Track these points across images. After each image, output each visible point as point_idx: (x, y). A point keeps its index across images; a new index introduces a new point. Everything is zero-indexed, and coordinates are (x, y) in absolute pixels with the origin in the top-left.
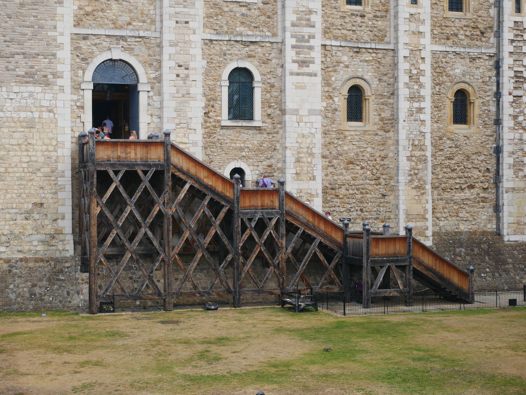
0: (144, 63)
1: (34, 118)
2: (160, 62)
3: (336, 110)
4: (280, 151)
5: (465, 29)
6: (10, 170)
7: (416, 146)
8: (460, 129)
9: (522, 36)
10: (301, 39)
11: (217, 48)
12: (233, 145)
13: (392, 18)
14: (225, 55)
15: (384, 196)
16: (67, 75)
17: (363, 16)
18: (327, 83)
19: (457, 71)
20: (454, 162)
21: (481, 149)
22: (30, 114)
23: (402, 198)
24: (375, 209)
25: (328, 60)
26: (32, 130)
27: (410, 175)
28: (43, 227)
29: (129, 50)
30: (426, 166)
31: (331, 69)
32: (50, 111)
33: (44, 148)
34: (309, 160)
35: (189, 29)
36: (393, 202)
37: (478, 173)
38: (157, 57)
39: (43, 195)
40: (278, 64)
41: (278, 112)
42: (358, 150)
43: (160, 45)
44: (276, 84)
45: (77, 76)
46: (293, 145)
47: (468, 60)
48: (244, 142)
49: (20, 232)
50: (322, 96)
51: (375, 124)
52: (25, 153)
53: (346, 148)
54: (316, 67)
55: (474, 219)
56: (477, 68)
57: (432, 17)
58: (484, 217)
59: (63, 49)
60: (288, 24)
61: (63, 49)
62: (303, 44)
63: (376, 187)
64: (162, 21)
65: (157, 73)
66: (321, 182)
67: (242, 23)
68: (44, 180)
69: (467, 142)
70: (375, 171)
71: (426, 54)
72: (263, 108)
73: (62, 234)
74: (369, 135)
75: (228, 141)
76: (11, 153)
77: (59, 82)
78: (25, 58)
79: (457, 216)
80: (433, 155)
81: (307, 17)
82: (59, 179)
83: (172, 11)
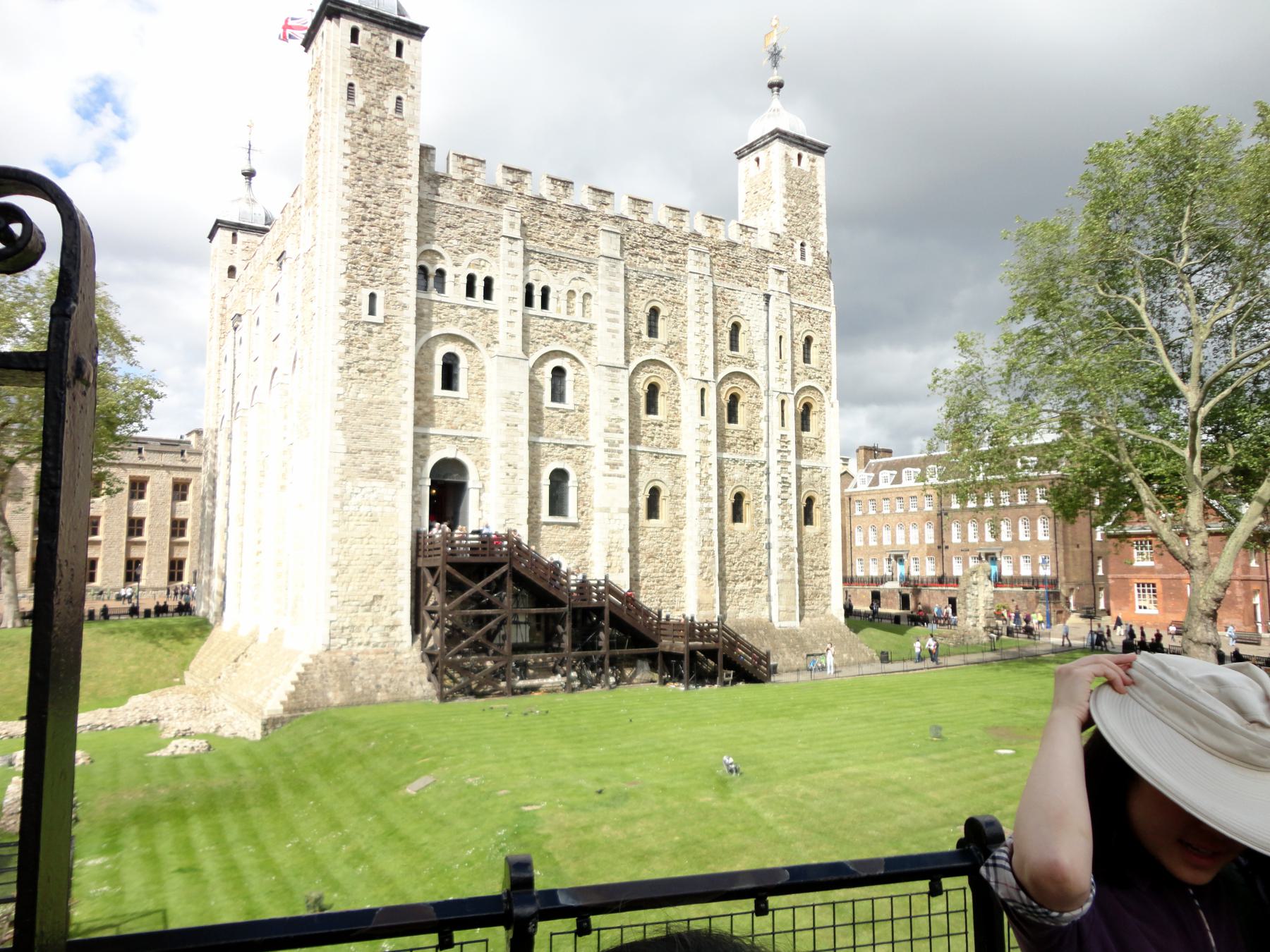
15: (678, 587)
18: (633, 484)
32: (393, 506)
34: (618, 554)
53: (646, 543)
54: (625, 470)
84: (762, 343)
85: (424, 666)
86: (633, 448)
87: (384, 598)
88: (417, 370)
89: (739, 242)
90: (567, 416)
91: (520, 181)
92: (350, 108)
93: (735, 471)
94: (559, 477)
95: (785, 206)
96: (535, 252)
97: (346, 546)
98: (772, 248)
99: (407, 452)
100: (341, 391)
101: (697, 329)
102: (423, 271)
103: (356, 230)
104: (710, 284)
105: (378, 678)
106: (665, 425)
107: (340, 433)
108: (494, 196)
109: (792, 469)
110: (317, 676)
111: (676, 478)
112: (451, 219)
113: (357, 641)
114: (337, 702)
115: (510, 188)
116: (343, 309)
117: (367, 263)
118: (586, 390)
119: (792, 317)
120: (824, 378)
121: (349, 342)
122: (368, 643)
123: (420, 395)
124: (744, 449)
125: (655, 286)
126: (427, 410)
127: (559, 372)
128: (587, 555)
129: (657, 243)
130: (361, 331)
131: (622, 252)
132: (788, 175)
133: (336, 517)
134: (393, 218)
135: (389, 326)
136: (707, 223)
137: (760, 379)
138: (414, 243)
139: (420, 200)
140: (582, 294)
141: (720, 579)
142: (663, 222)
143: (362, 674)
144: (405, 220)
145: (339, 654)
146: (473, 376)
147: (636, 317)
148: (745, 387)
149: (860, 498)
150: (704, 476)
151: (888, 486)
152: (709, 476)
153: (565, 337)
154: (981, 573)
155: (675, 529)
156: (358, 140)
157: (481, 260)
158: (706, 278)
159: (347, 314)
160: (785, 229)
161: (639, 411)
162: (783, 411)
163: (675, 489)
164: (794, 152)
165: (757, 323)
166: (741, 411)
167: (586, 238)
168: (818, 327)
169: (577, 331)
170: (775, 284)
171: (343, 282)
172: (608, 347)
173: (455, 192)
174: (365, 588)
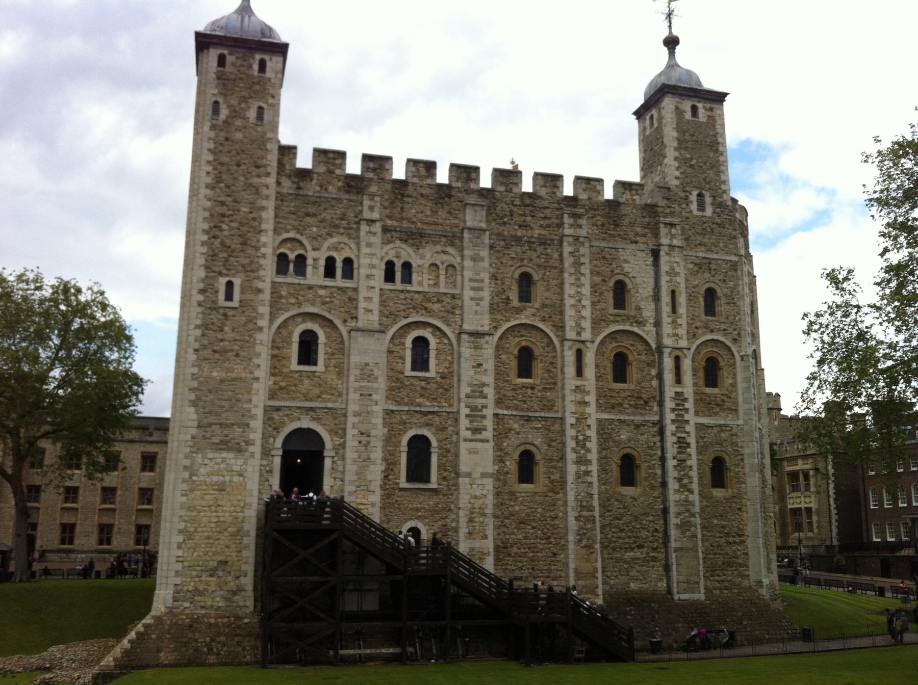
0: (330, 431)
1: (225, 482)
2: (344, 430)
3: (507, 473)
4: (454, 512)
5: (629, 399)
6: (200, 529)
7: (584, 506)
8: (629, 491)
9: (683, 405)
10: (474, 408)
11: (398, 417)
12: (410, 506)
13: (560, 390)
14: (405, 423)
15: (555, 555)
16: (258, 443)
17: (533, 388)
18: (498, 448)
19: (622, 437)
20: (622, 522)
21: (649, 511)
22: (221, 478)
23: (572, 557)
24: (546, 568)
25: (500, 427)
26: (222, 492)
27: (578, 535)
28: (226, 583)
29: (318, 420)
30: (595, 525)
31: (503, 436)
32: (241, 475)
33: (232, 509)
34: (481, 519)
35: (371, 400)
36: (563, 561)
37: (647, 533)
38: (342, 426)
39: (228, 554)
40: (454, 432)
41: (453, 475)
42: (529, 511)
43: (345, 415)
44: (451, 449)
45: (269, 443)
46: (466, 505)
47: (632, 427)
49: (204, 589)
50: (494, 460)
51: (546, 486)
52: (215, 514)
53: (517, 508)
54: (488, 434)
55: (645, 578)
56: (642, 434)
57: (597, 388)
59: (256, 419)
60: (463, 396)
61: (256, 419)
62: (476, 413)
63: (547, 546)
64: (347, 394)
65: (342, 440)
66: (492, 540)
67: (422, 395)
68: (231, 539)
69: (635, 503)
70: (545, 530)
71: (592, 421)
72: (438, 471)
73: (244, 590)
74: (540, 496)
75: (405, 502)
76: (202, 514)
77: (251, 449)
78: (221, 427)
79: (628, 575)
80: (600, 516)
81: (481, 389)
82: (244, 538)
83: (357, 385)
84: (651, 299)
87: (229, 563)
88: (273, 348)
89: (622, 200)
90: (428, 383)
91: (381, 167)
92: (215, 122)
93: (622, 432)
94: (419, 446)
95: (676, 159)
99: (257, 424)
100: (195, 370)
102: (282, 259)
103: (215, 227)
104: (587, 245)
107: (192, 410)
108: (354, 184)
109: (691, 428)
112: (312, 209)
115: (371, 175)
116: (201, 298)
117: (225, 255)
120: (730, 330)
121: (205, 326)
122: (212, 606)
126: (283, 384)
127: (421, 344)
129: (527, 210)
130: (215, 317)
131: (488, 222)
132: (680, 127)
134: (251, 212)
135: (244, 309)
136: (584, 186)
138: (271, 233)
140: (445, 266)
144: (264, 215)
146: (330, 351)
147: (503, 283)
148: (632, 345)
150: (581, 438)
153: (426, 309)
155: (550, 494)
156: (220, 148)
157: (340, 243)
158: (581, 240)
159: (204, 301)
160: (677, 182)
161: (508, 376)
164: (687, 105)
168: (721, 277)
169: (439, 301)
173: (317, 184)
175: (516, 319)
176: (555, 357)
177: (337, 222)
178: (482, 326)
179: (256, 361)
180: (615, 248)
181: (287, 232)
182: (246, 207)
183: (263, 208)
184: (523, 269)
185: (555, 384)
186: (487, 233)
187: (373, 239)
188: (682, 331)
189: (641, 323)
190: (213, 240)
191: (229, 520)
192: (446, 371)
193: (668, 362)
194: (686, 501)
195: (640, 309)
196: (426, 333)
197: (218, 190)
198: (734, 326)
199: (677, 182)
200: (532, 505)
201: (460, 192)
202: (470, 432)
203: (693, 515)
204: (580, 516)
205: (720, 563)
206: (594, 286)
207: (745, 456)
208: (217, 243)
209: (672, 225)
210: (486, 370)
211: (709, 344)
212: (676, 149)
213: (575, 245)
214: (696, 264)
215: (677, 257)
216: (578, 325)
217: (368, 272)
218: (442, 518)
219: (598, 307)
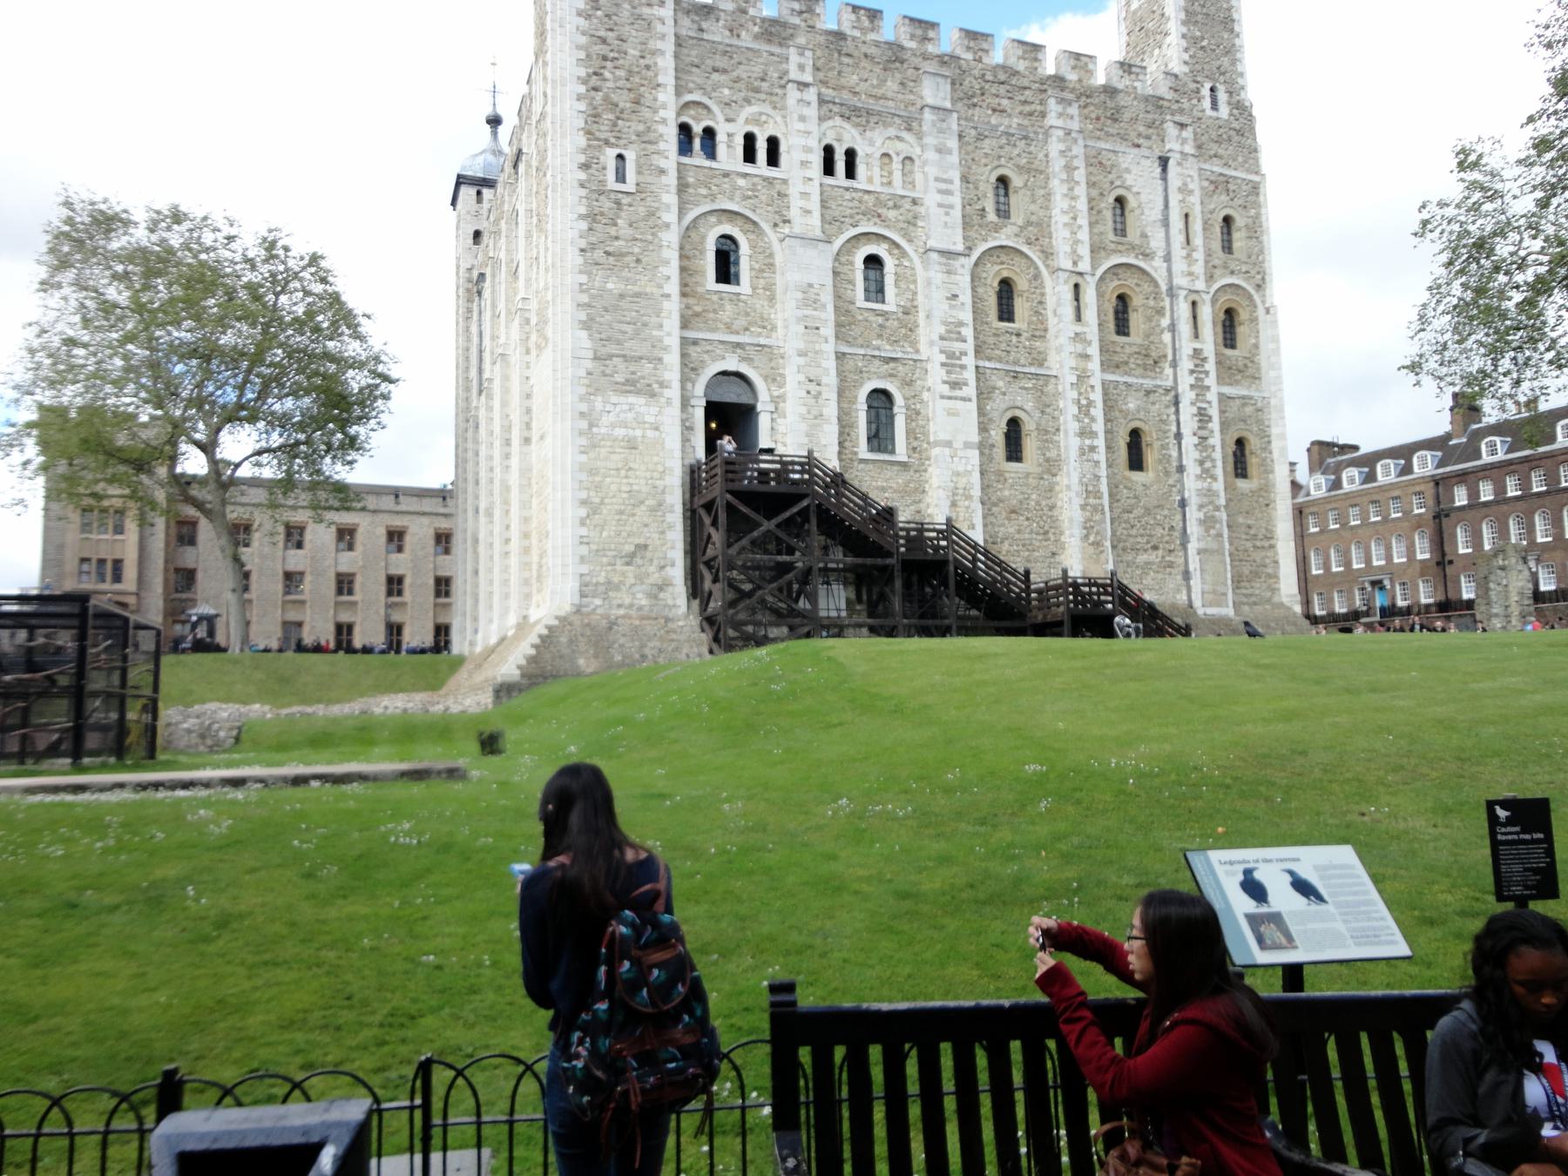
0: (766, 378)
3: (993, 446)
8: (1137, 476)
14: (861, 372)
16: (676, 385)
17: (1018, 335)
18: (981, 412)
20: (1132, 516)
27: (1085, 528)
32: (657, 429)
33: (648, 475)
34: (967, 503)
48: (887, 480)
51: (1040, 465)
52: (625, 481)
53: (1007, 493)
54: (970, 390)
56: (1153, 403)
58: (1171, 586)
67: (880, 336)
77: (667, 393)
83: (800, 313)
84: (1159, 224)
85: (704, 636)
86: (981, 363)
87: (650, 548)
88: (682, 257)
89: (1120, 86)
93: (1129, 399)
95: (1184, 36)
96: (834, 103)
97: (598, 479)
98: (1169, 95)
99: (673, 359)
101: (1065, 204)
102: (685, 129)
103: (595, 74)
104: (1081, 142)
105: (643, 646)
106: (1025, 335)
107: (584, 334)
109: (1212, 396)
110: (564, 640)
111: (1046, 405)
112: (721, 62)
113: (616, 602)
114: (590, 670)
115: (796, 20)
116: (582, 176)
117: (611, 116)
118: (912, 287)
119: (1202, 188)
120: (1253, 272)
121: (592, 217)
122: (631, 606)
123: (688, 289)
124: (1140, 371)
125: (1001, 147)
126: (698, 309)
127: (873, 262)
128: (922, 506)
129: (1002, 89)
130: (606, 204)
131: (954, 101)
133: (583, 441)
134: (643, 57)
135: (643, 195)
136: (1072, 62)
137: (1160, 276)
138: (671, 90)
139: (676, 35)
140: (901, 158)
141: (1114, 547)
142: (1012, 61)
143: (622, 641)
144: (660, 61)
145: (593, 617)
146: (757, 266)
148: (1138, 285)
149: (1312, 509)
150: (1084, 402)
151: (1356, 487)
152: (1090, 403)
153: (879, 216)
154: (1511, 552)
157: (761, 114)
158: (1074, 135)
159: (589, 181)
160: (1186, 69)
161: (987, 315)
162: (1195, 317)
163: (1043, 422)
165: (1151, 197)
166: (1136, 320)
167: (902, 84)
168: (1241, 202)
169: (896, 207)
170: (1176, 142)
171: (582, 141)
172: (943, 228)
173: (725, 27)
174: (624, 534)
175: (995, 239)
176: (1043, 295)
177: (756, 84)
178: (954, 244)
179: (664, 270)
180: (1114, 151)
181: (690, 92)
182: (635, 49)
183: (654, 53)
184: (1001, 171)
185: (1046, 330)
186: (955, 115)
187: (807, 111)
188: (1199, 268)
189: (1147, 256)
190: (593, 93)
191: (644, 489)
192: (909, 304)
193: (1184, 309)
194: (1209, 490)
195: (1146, 236)
196: (880, 250)
197: (595, 21)
198: (1257, 269)
199: (1186, 69)
200: (1024, 489)
201: (915, 55)
202: (947, 386)
203: (1217, 509)
204: (1086, 505)
205: (1247, 572)
206: (1090, 200)
207: (1273, 438)
208: (599, 96)
209: (1182, 126)
210: (963, 304)
211: (1229, 290)
212: (1184, 23)
213: (1064, 141)
214: (1212, 182)
215: (1192, 167)
216: (1074, 251)
217: (804, 157)
218: (915, 502)
219: (1096, 231)
